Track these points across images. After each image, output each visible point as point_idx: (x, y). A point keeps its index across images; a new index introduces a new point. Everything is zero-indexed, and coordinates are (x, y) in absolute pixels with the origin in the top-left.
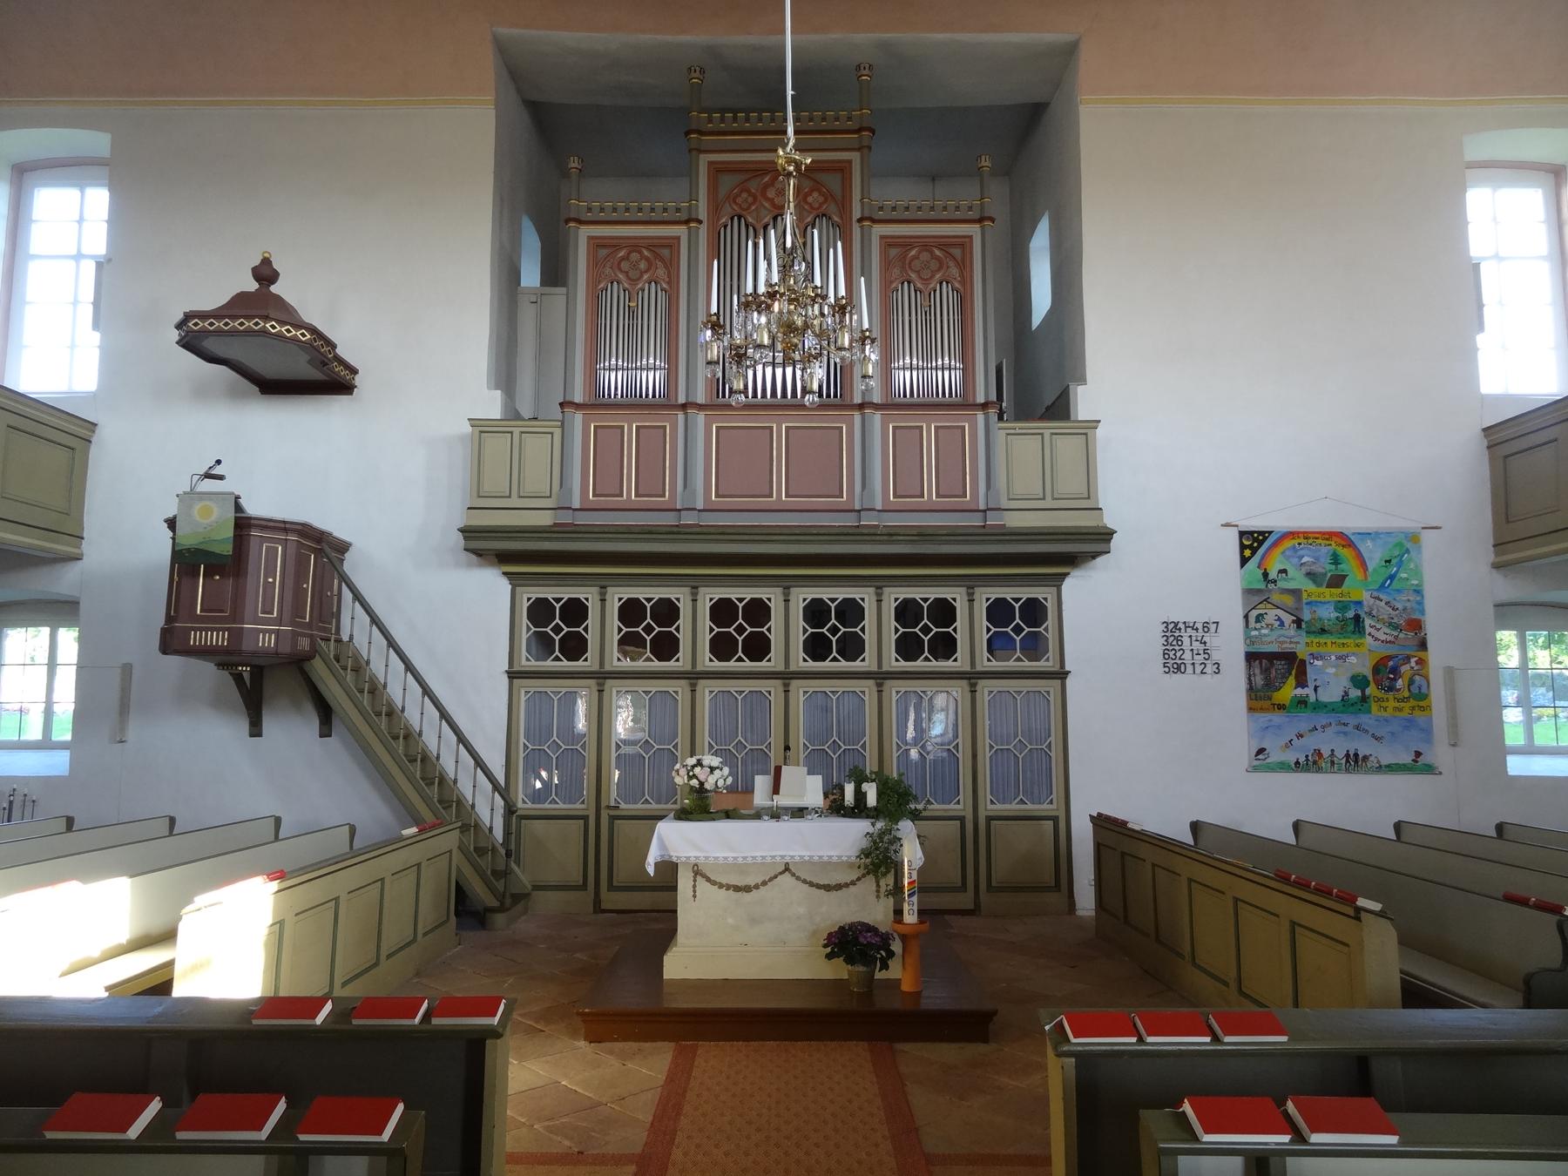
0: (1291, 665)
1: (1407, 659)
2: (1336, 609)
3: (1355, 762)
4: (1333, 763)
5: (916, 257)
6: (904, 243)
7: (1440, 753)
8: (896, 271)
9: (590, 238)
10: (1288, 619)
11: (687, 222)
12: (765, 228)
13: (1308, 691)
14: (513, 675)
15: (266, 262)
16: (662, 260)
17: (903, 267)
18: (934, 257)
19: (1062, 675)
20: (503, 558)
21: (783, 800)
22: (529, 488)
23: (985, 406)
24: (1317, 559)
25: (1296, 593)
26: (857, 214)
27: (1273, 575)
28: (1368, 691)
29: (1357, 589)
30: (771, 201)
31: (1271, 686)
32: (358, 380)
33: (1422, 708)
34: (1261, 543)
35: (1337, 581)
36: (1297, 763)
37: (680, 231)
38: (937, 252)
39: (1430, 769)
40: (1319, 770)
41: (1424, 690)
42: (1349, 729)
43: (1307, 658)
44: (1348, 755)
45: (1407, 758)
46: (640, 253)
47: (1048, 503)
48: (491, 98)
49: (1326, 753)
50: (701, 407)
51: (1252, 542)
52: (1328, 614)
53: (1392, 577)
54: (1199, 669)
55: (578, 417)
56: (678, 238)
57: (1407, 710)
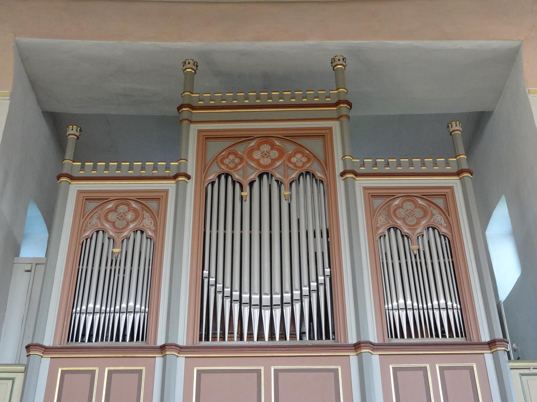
6: (388, 195)
8: (381, 219)
9: (80, 192)
11: (175, 177)
12: (251, 184)
16: (149, 210)
17: (389, 216)
18: (416, 205)
23: (492, 344)
26: (339, 168)
30: (257, 162)
37: (169, 185)
38: (420, 202)
46: (128, 205)
48: (7, 92)
50: (181, 349)
55: (46, 362)
56: (167, 191)
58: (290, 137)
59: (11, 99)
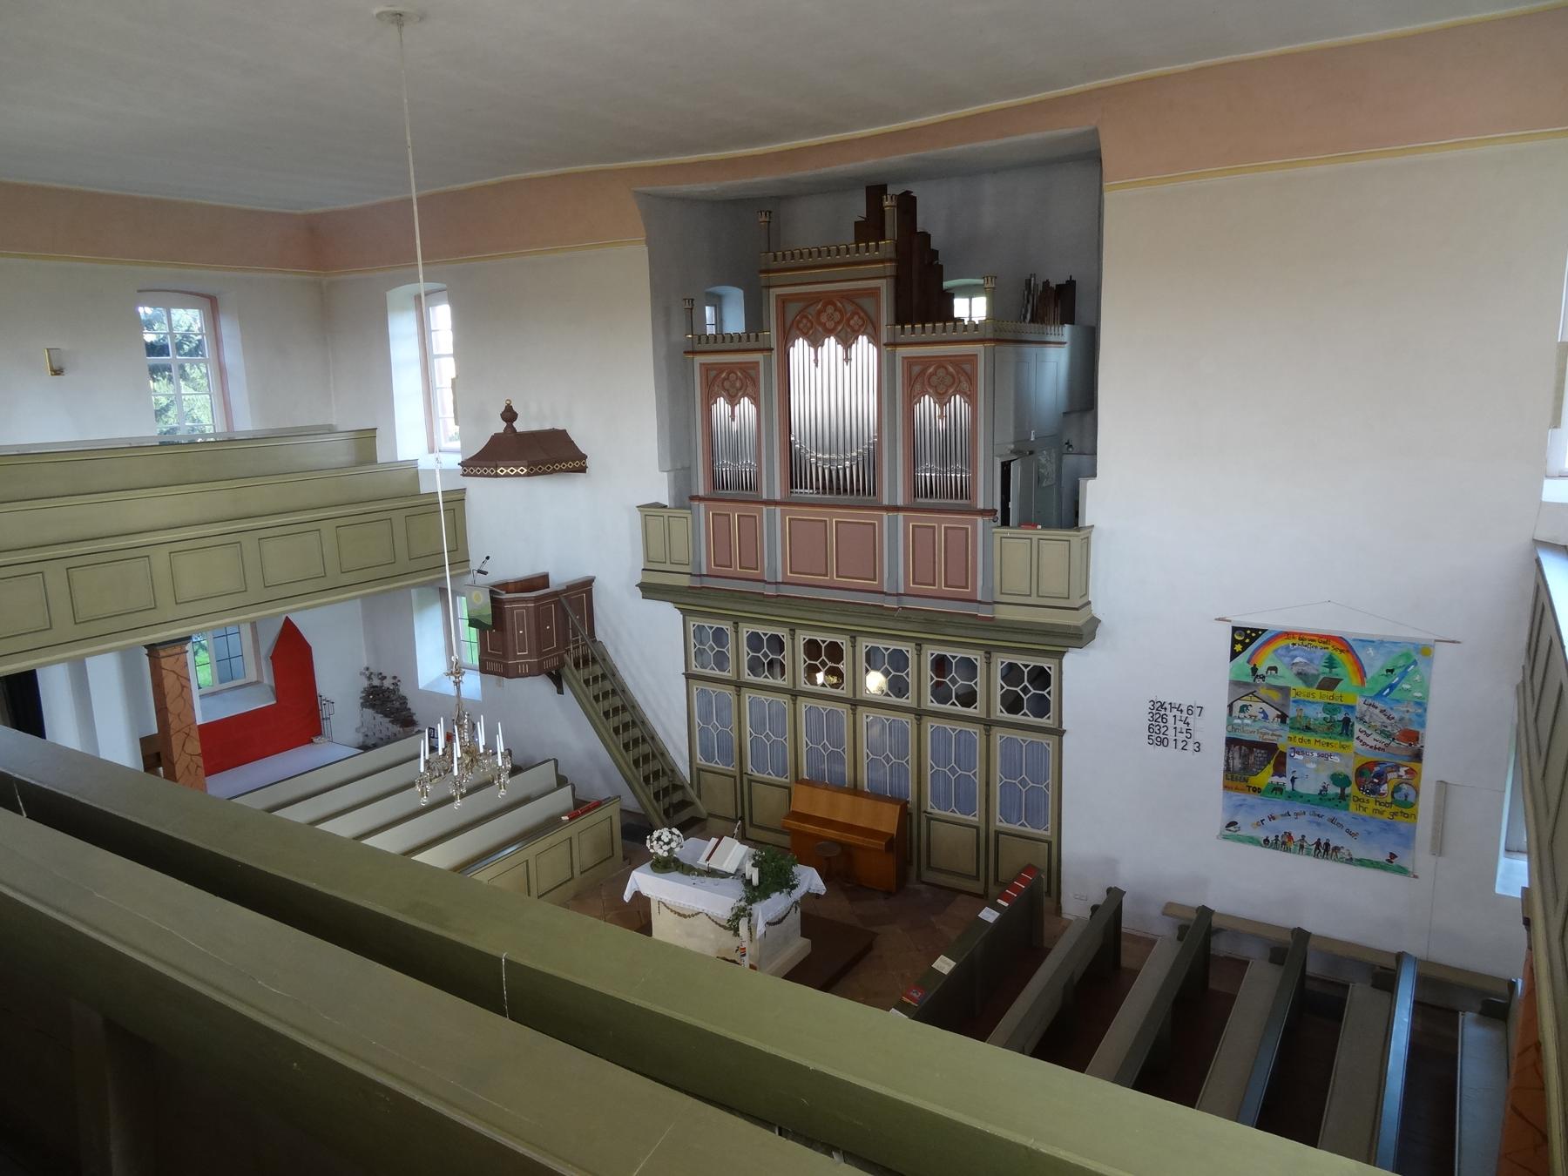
0: (1274, 756)
1: (1397, 767)
2: (1325, 710)
3: (1324, 850)
4: (1302, 847)
5: (934, 374)
7: (1421, 857)
10: (1272, 713)
13: (1285, 781)
14: (689, 676)
19: (1059, 733)
21: (713, 864)
22: (676, 558)
23: (983, 512)
24: (1311, 661)
25: (1284, 691)
27: (1262, 670)
28: (1348, 791)
29: (1350, 692)
31: (1248, 770)
33: (1406, 816)
34: (1253, 640)
35: (1330, 684)
36: (1266, 840)
39: (1402, 871)
40: (1288, 850)
41: (1411, 799)
42: (1324, 820)
43: (1288, 751)
44: (1318, 843)
45: (1382, 857)
47: (1033, 600)
49: (1296, 837)
50: (776, 503)
51: (1245, 638)
52: (1316, 714)
53: (1392, 687)
54: (1180, 745)
57: (1386, 815)
58: (849, 296)
59: (648, 242)
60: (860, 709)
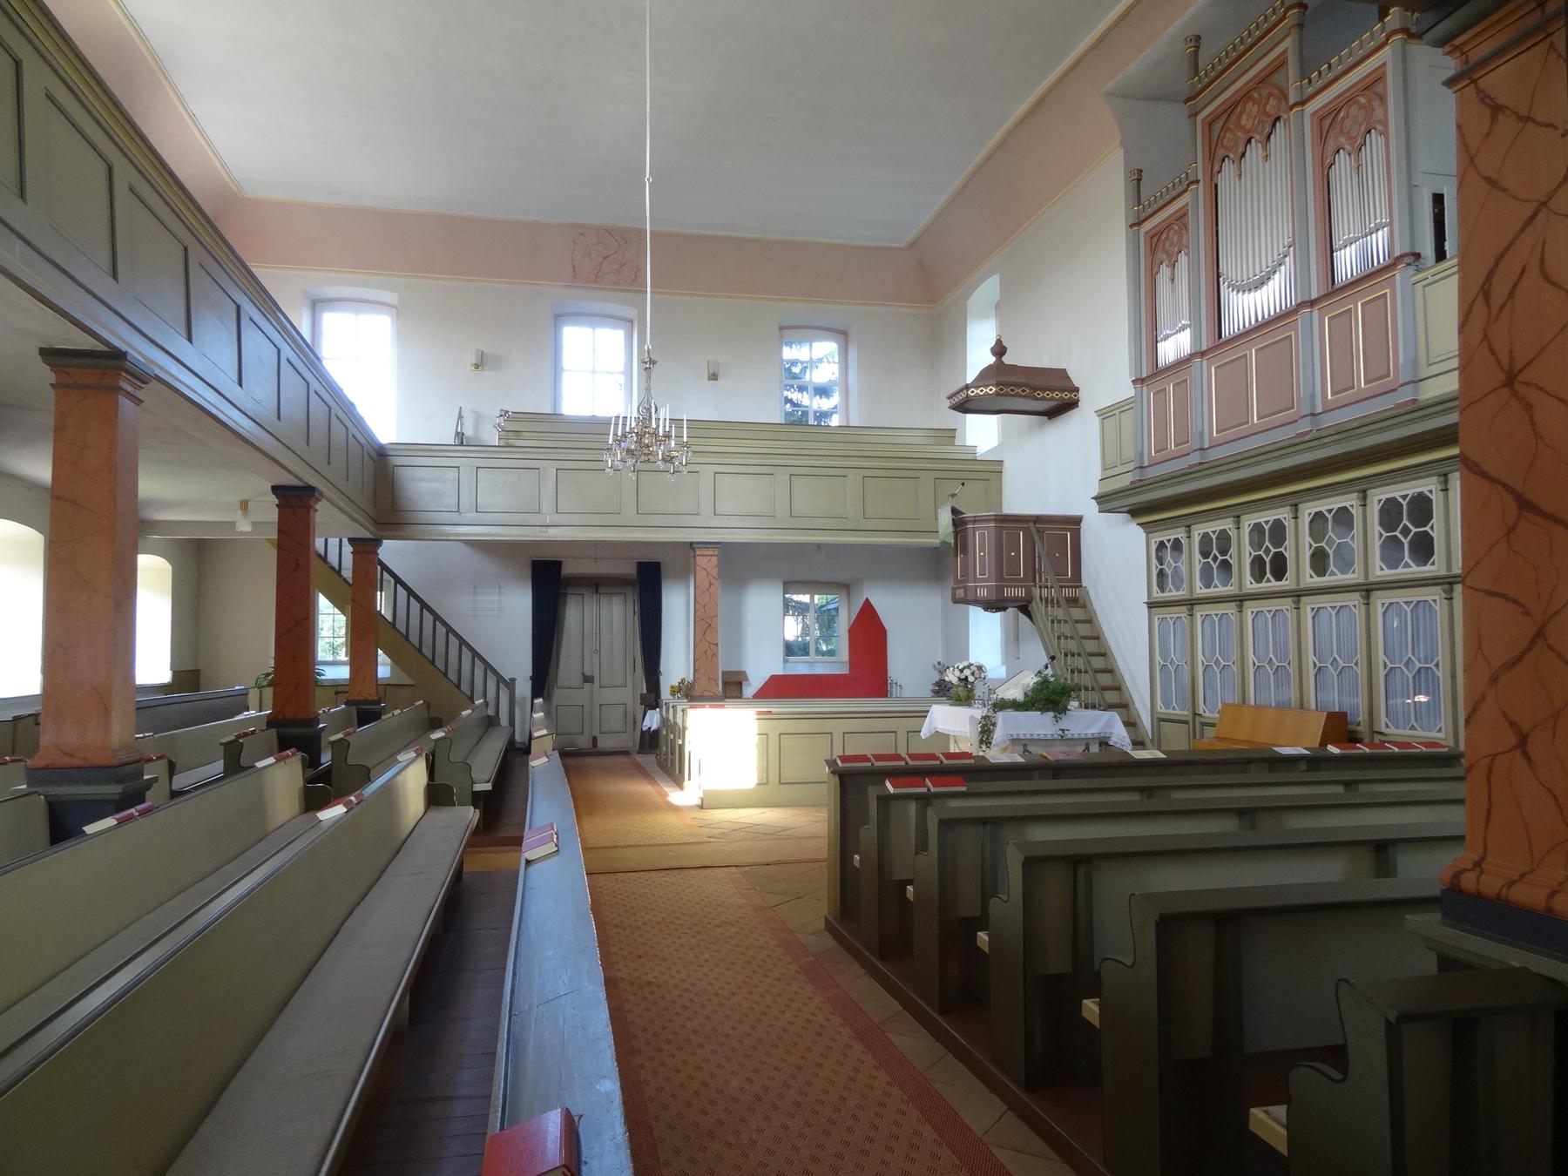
5: (1344, 118)
14: (1152, 605)
15: (999, 342)
18: (1362, 107)
20: (1135, 512)
32: (1082, 395)
59: (1124, 144)
60: (1304, 599)
